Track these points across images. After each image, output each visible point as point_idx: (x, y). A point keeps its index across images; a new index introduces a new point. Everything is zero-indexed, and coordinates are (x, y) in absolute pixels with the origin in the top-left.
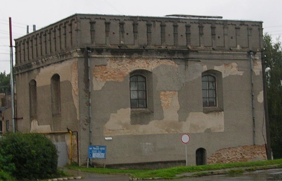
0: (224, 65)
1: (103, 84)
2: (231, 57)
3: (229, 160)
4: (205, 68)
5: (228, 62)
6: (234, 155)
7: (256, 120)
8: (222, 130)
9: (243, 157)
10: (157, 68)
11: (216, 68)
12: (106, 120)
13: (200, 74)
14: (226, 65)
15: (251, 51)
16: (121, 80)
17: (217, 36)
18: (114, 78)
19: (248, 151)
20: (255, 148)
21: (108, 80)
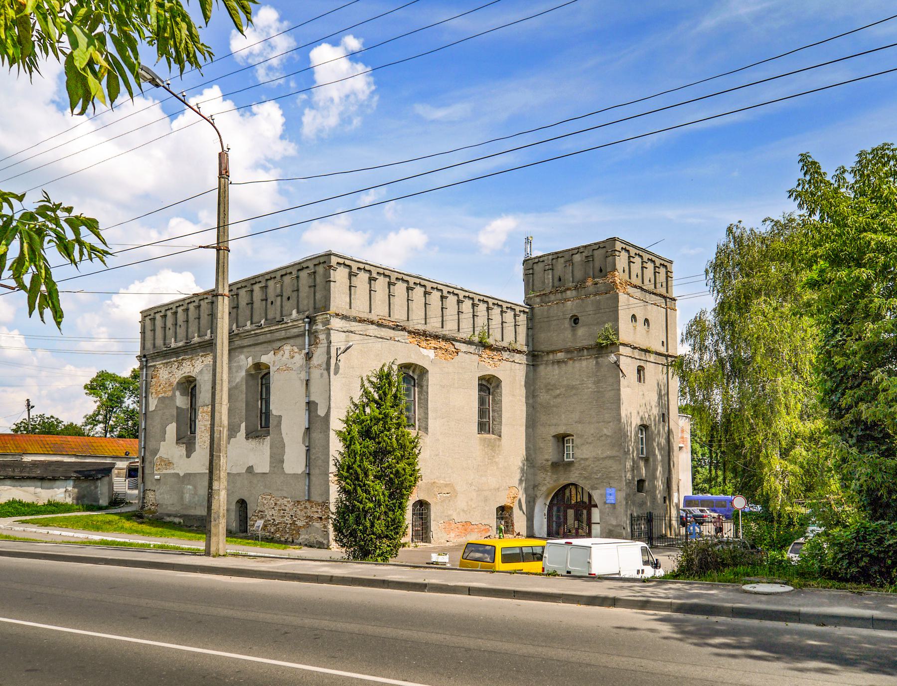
0: (272, 352)
1: (156, 402)
2: (283, 334)
3: (275, 525)
4: (250, 361)
5: (278, 344)
6: (282, 517)
7: (313, 451)
8: (266, 469)
9: (294, 523)
10: (201, 372)
11: (264, 359)
12: (156, 451)
13: (243, 373)
14: (276, 350)
15: (307, 317)
16: (170, 394)
17: (269, 301)
18: (165, 392)
19: (301, 510)
20: (312, 507)
21: (160, 396)
